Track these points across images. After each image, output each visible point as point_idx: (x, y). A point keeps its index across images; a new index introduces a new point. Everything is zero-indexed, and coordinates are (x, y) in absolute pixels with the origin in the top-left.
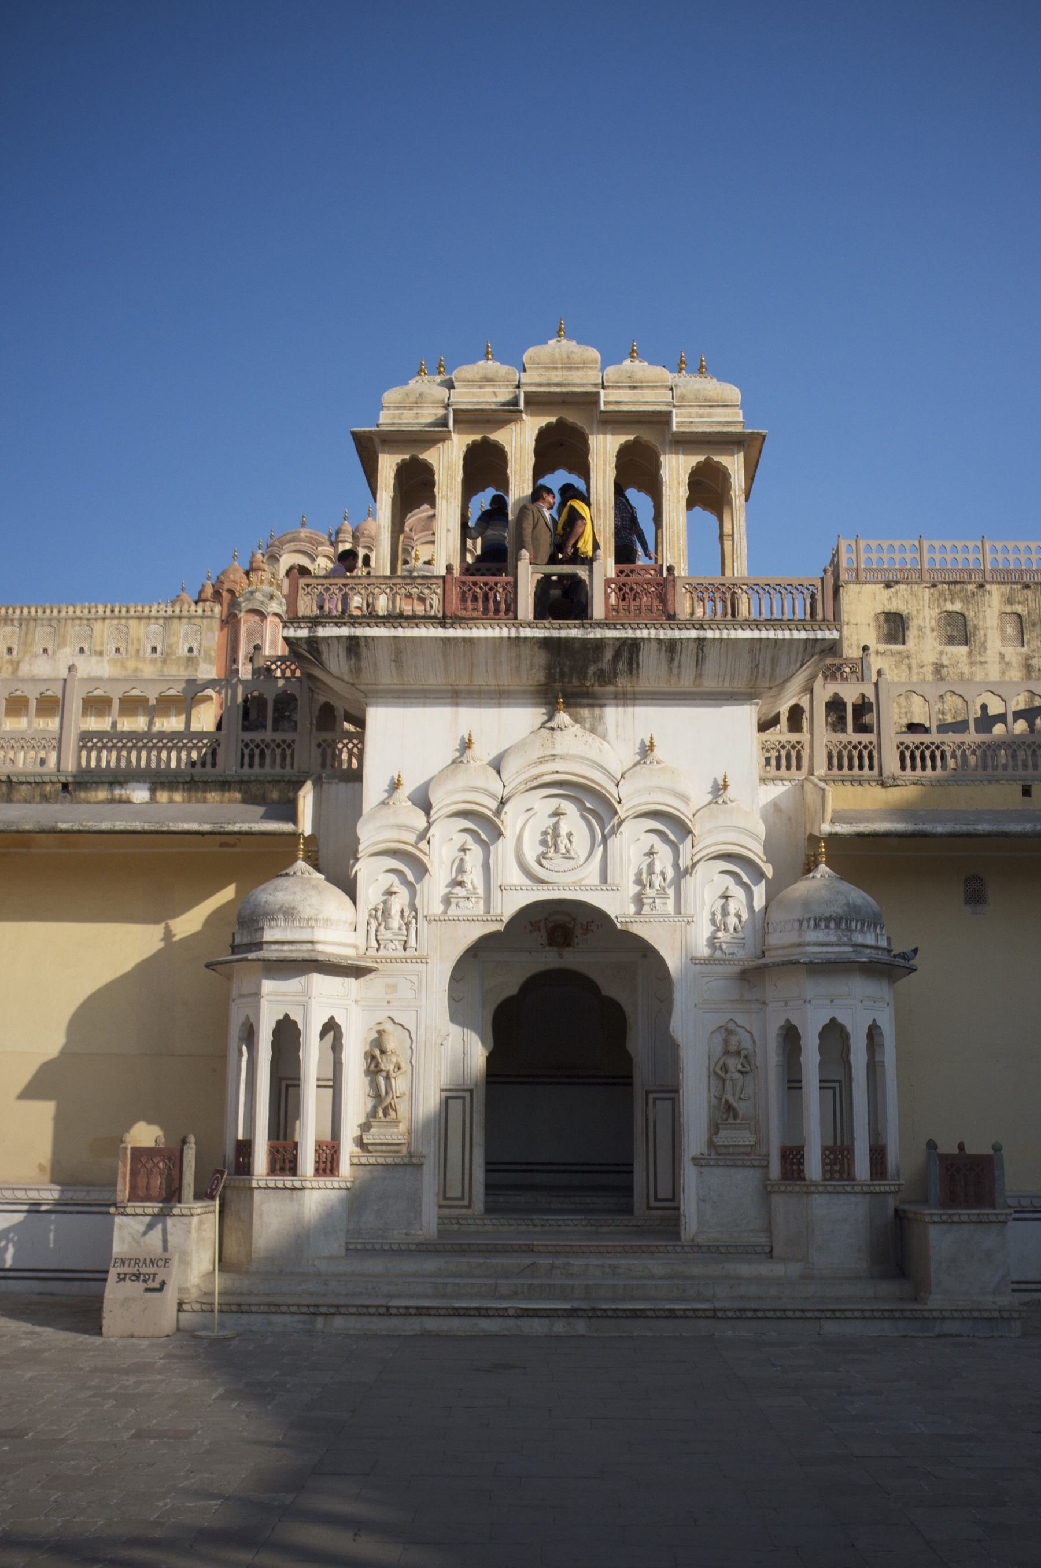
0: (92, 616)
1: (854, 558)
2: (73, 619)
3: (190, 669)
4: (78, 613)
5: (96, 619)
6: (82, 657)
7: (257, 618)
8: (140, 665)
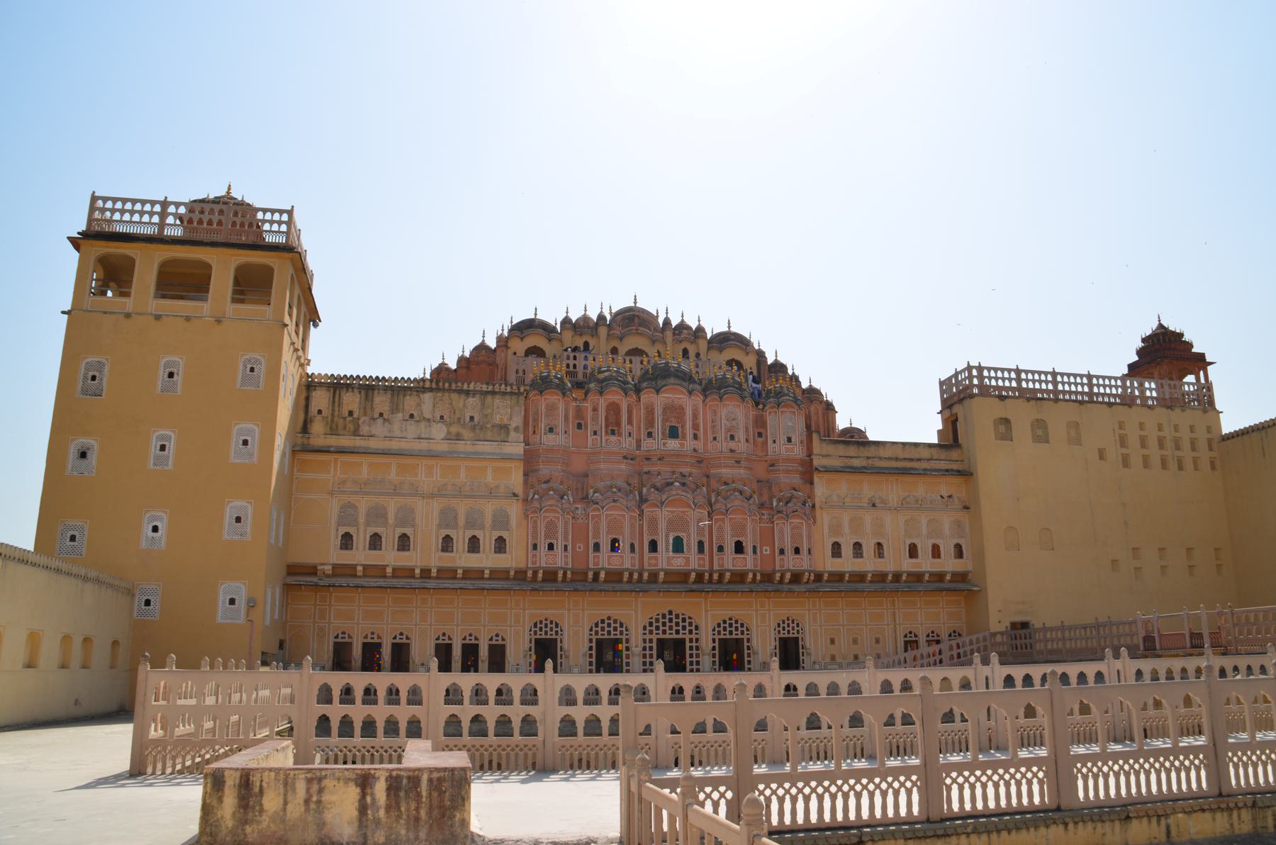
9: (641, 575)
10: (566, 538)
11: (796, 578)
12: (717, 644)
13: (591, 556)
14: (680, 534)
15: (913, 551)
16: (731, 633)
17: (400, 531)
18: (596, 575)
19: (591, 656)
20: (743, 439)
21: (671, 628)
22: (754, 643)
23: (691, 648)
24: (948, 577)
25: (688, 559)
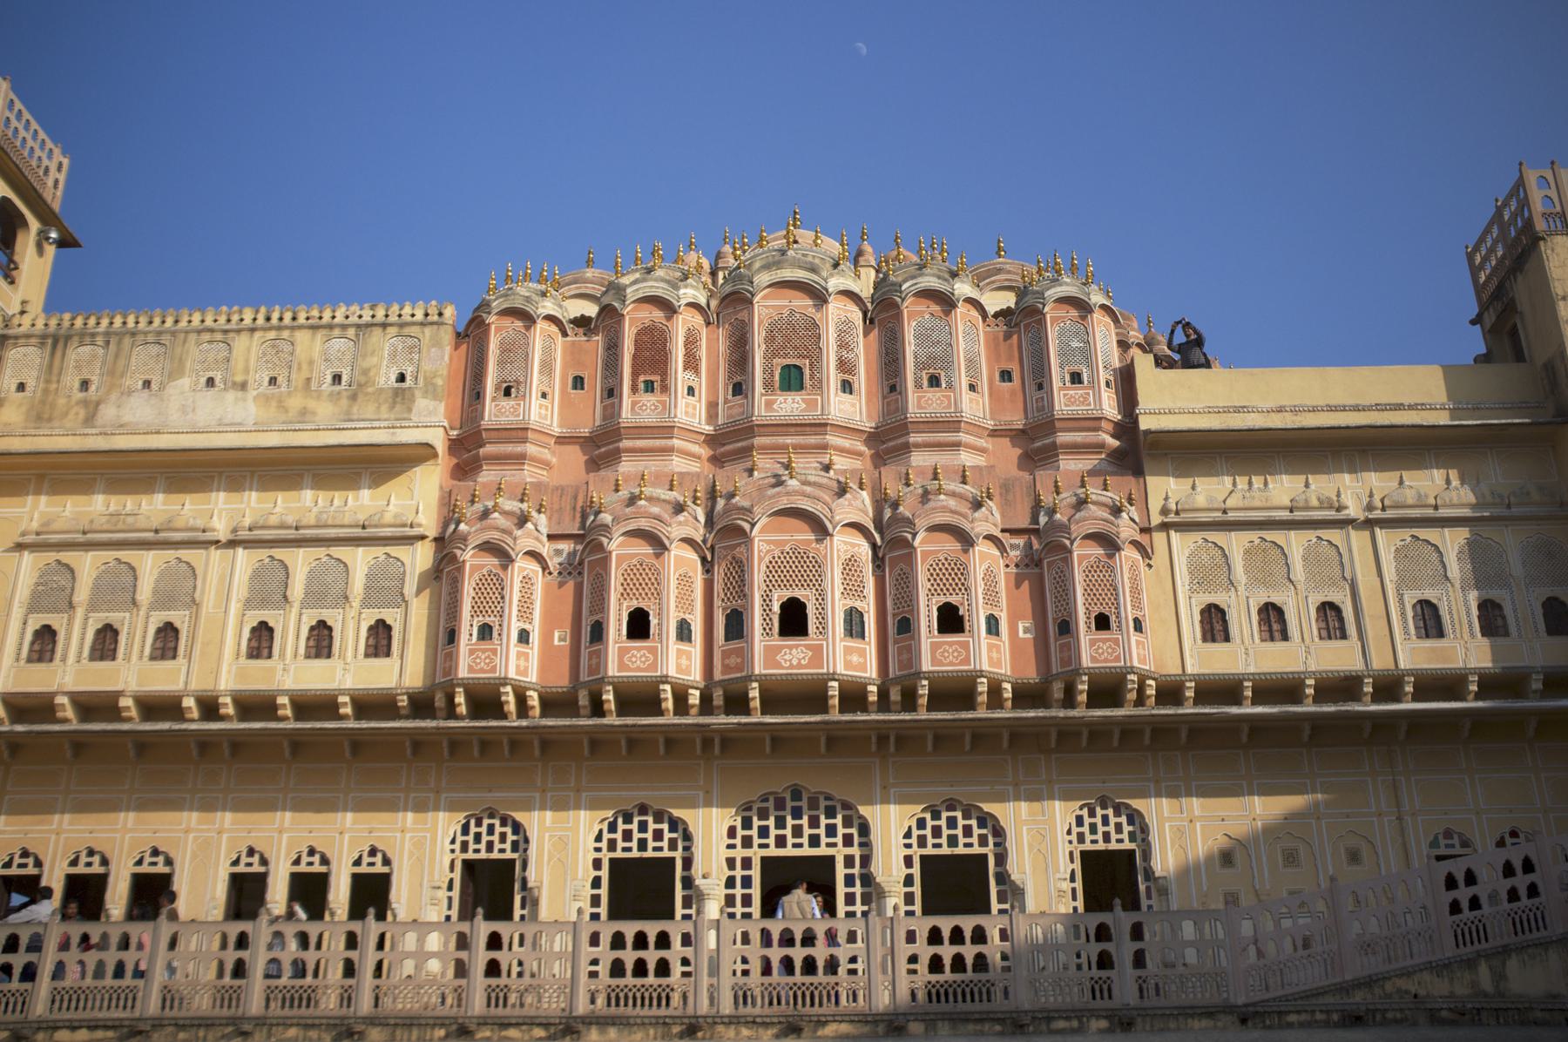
0: (233, 325)
1: (1553, 194)
2: (199, 332)
3: (398, 407)
4: (209, 322)
5: (239, 331)
6: (212, 392)
7: (519, 324)
8: (311, 404)
10: (525, 613)
11: (1108, 689)
12: (916, 870)
13: (584, 654)
14: (799, 593)
16: (953, 841)
17: (157, 619)
19: (595, 900)
23: (849, 881)
24: (1537, 685)
25: (817, 650)
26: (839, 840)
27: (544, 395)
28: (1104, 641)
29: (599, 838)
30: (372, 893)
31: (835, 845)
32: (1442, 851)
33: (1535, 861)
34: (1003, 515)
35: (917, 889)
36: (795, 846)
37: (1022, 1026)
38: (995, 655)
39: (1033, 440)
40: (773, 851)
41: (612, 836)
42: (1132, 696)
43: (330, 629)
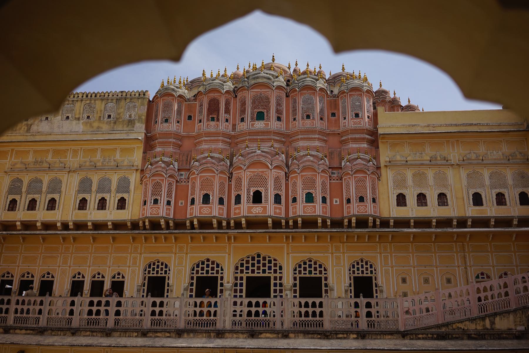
0: (75, 99)
3: (130, 126)
6: (68, 121)
8: (101, 125)
9: (228, 223)
10: (169, 195)
11: (362, 223)
12: (298, 282)
13: (189, 208)
14: (259, 189)
15: (477, 200)
16: (310, 272)
17: (50, 196)
18: (192, 223)
19: (191, 290)
20: (317, 116)
21: (259, 268)
22: (330, 281)
23: (275, 285)
24: (515, 222)
25: (265, 208)
26: (272, 271)
27: (178, 122)
28: (362, 206)
29: (193, 270)
30: (118, 287)
31: (271, 273)
32: (480, 279)
33: (508, 284)
34: (330, 163)
35: (298, 288)
36: (257, 273)
37: (327, 336)
38: (325, 210)
39: (342, 137)
40: (250, 275)
41: (198, 269)
42: (371, 224)
43: (106, 200)
